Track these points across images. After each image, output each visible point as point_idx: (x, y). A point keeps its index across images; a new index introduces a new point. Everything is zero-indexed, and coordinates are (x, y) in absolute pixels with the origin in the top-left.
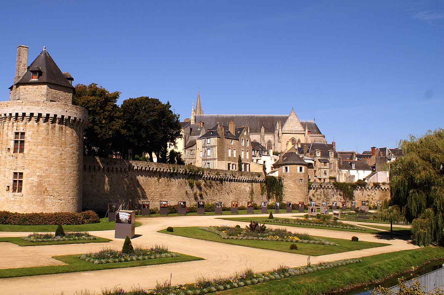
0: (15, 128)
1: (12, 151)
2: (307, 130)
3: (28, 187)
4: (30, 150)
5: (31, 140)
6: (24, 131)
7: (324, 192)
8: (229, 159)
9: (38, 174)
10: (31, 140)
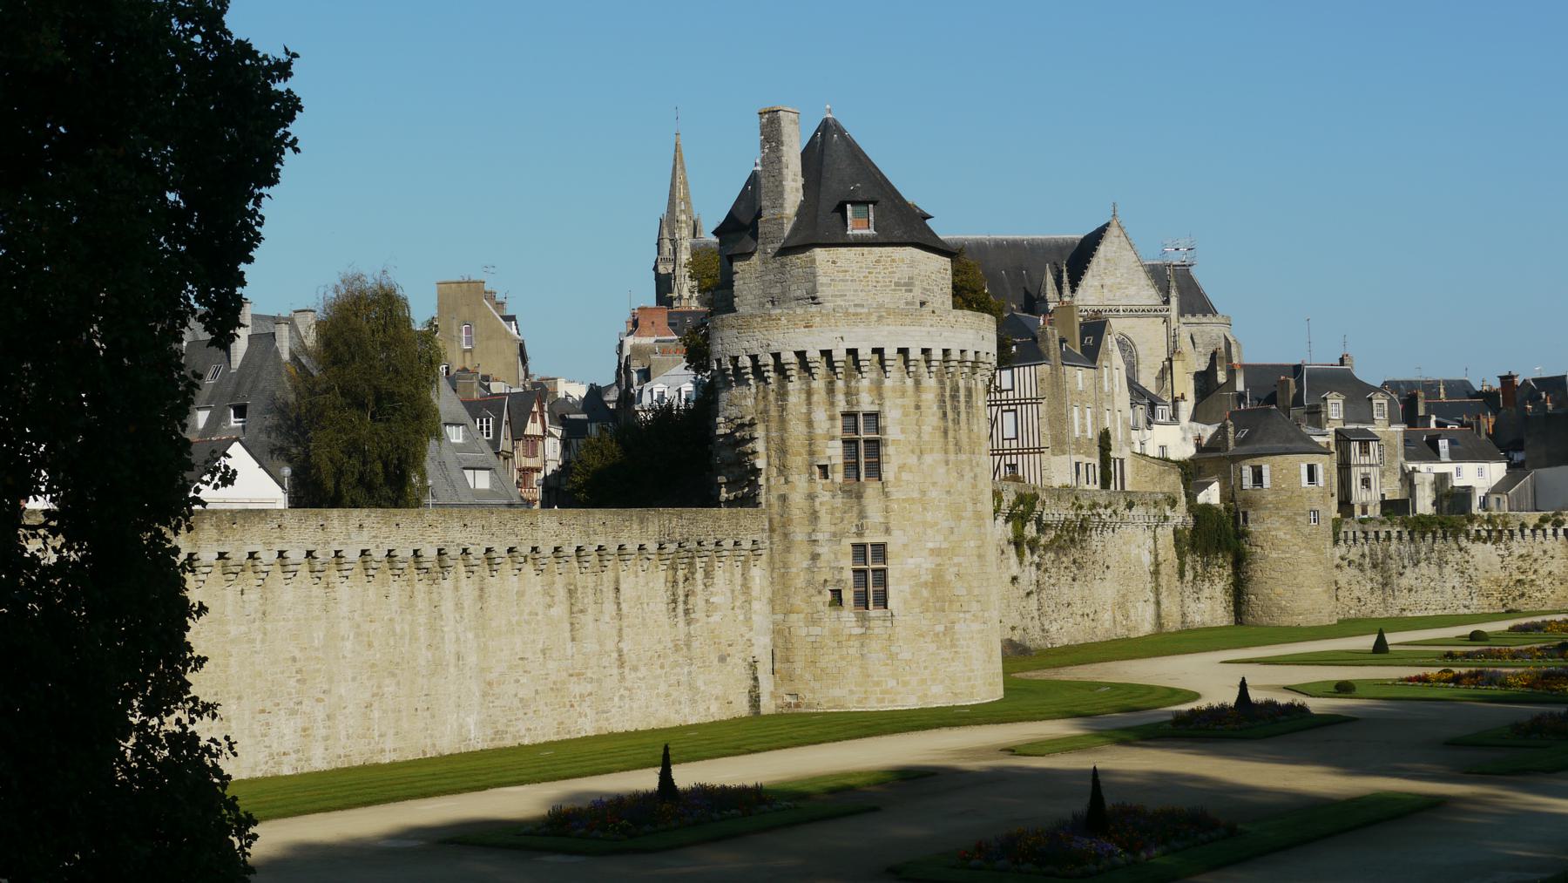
0: (840, 399)
2: (1174, 301)
3: (906, 588)
4: (902, 468)
5: (901, 437)
6: (875, 408)
7: (1373, 554)
8: (1079, 445)
9: (930, 545)
10: (901, 437)
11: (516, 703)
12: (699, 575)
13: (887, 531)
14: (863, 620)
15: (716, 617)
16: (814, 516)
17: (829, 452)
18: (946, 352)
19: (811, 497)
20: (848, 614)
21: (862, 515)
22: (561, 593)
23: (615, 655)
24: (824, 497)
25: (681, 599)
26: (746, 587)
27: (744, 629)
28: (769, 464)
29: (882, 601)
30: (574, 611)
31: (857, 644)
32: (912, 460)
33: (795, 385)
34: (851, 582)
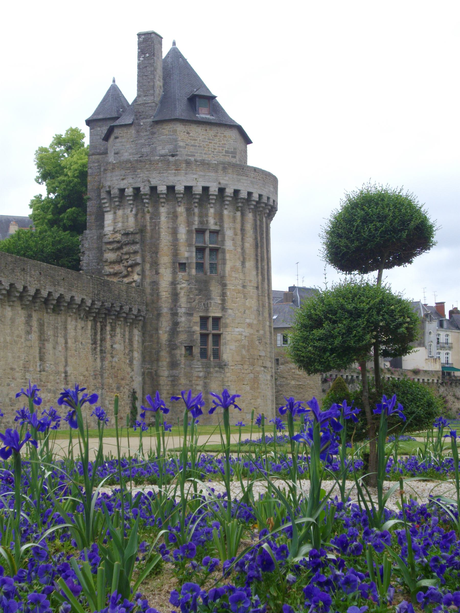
1: (194, 272)
4: (233, 269)
6: (217, 228)
9: (248, 321)
11: (7, 400)
12: (108, 328)
13: (224, 309)
14: (207, 366)
15: (116, 359)
16: (175, 296)
17: (187, 255)
18: (260, 196)
19: (174, 283)
20: (198, 364)
21: (208, 297)
22: (35, 324)
23: (63, 375)
24: (183, 286)
25: (99, 342)
26: (131, 341)
27: (129, 370)
28: (144, 261)
29: (217, 354)
30: (42, 340)
31: (201, 383)
32: (238, 264)
33: (163, 210)
34: (199, 341)
